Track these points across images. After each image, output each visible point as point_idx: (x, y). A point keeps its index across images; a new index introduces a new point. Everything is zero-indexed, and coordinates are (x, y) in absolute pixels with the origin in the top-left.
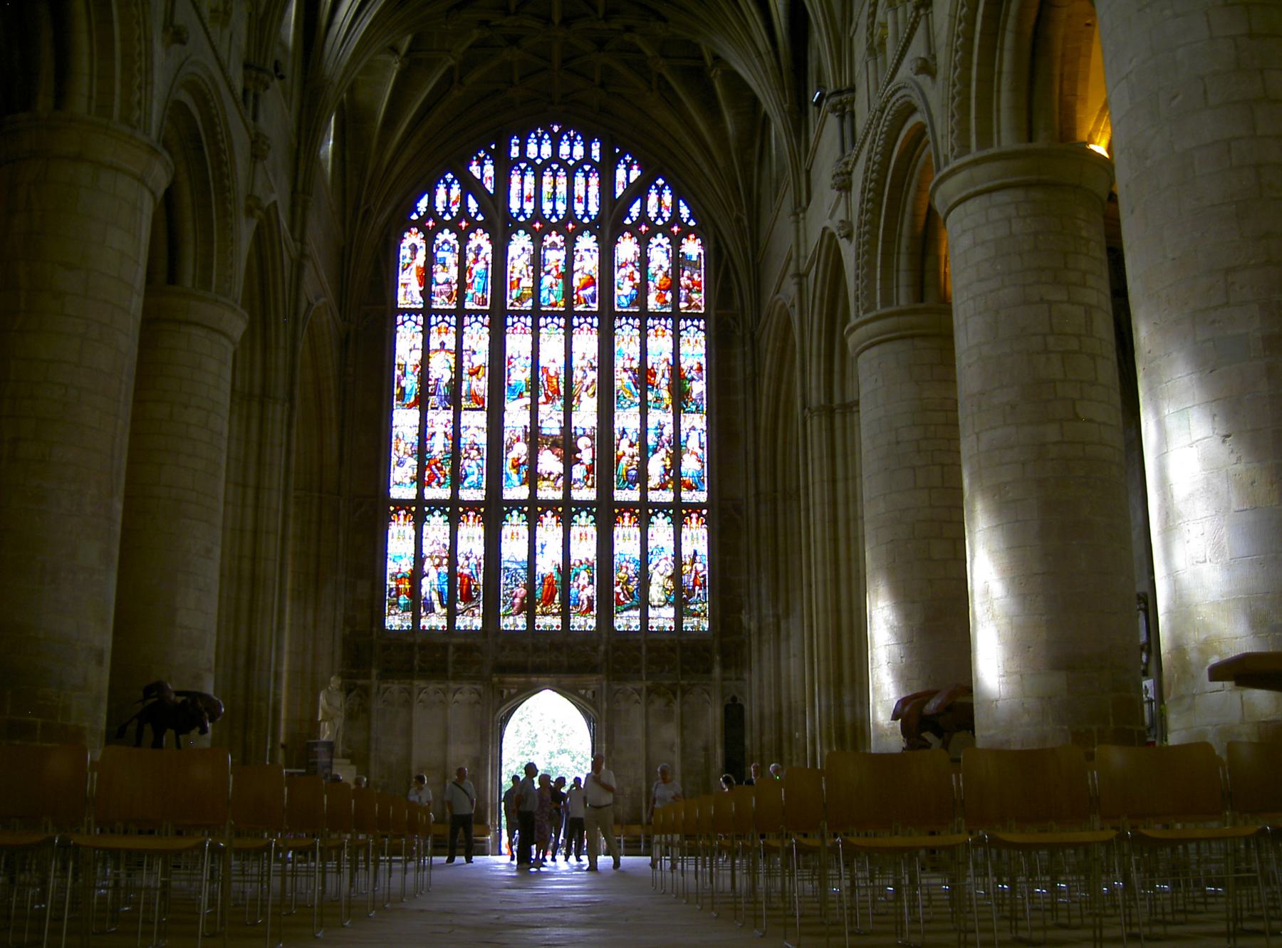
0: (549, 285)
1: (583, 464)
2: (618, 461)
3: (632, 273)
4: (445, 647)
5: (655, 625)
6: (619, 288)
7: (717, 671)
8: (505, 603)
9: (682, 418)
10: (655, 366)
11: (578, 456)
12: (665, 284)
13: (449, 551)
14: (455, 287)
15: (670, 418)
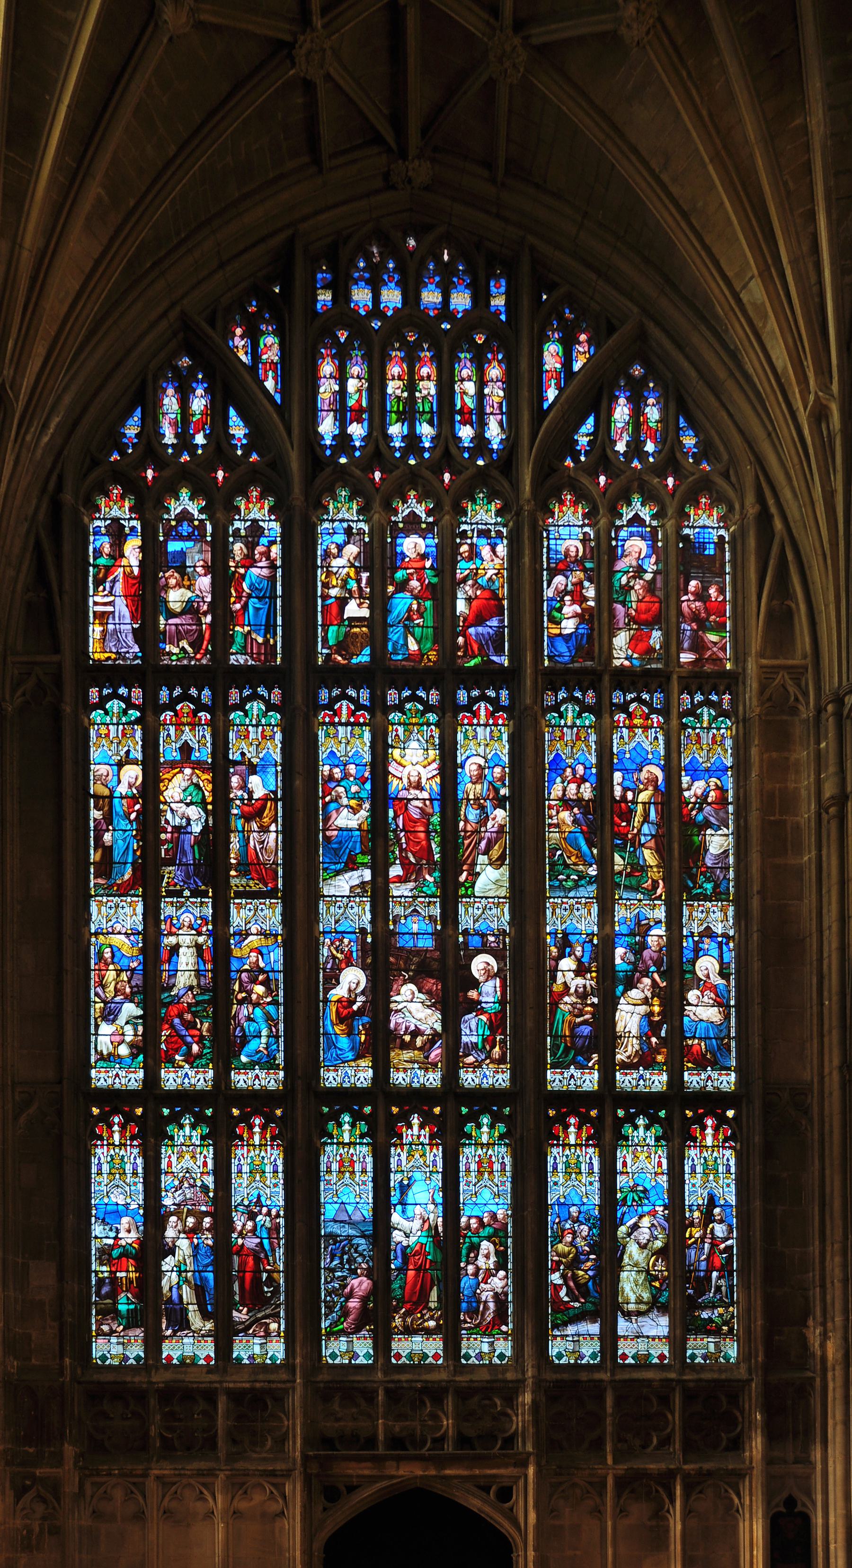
0: (404, 614)
1: (482, 1011)
2: (555, 1005)
3: (579, 584)
4: (210, 1396)
5: (631, 1352)
6: (552, 620)
7: (757, 1446)
8: (330, 1309)
9: (686, 911)
10: (630, 795)
11: (473, 994)
12: (648, 610)
13: (215, 1200)
14: (209, 619)
15: (660, 913)
